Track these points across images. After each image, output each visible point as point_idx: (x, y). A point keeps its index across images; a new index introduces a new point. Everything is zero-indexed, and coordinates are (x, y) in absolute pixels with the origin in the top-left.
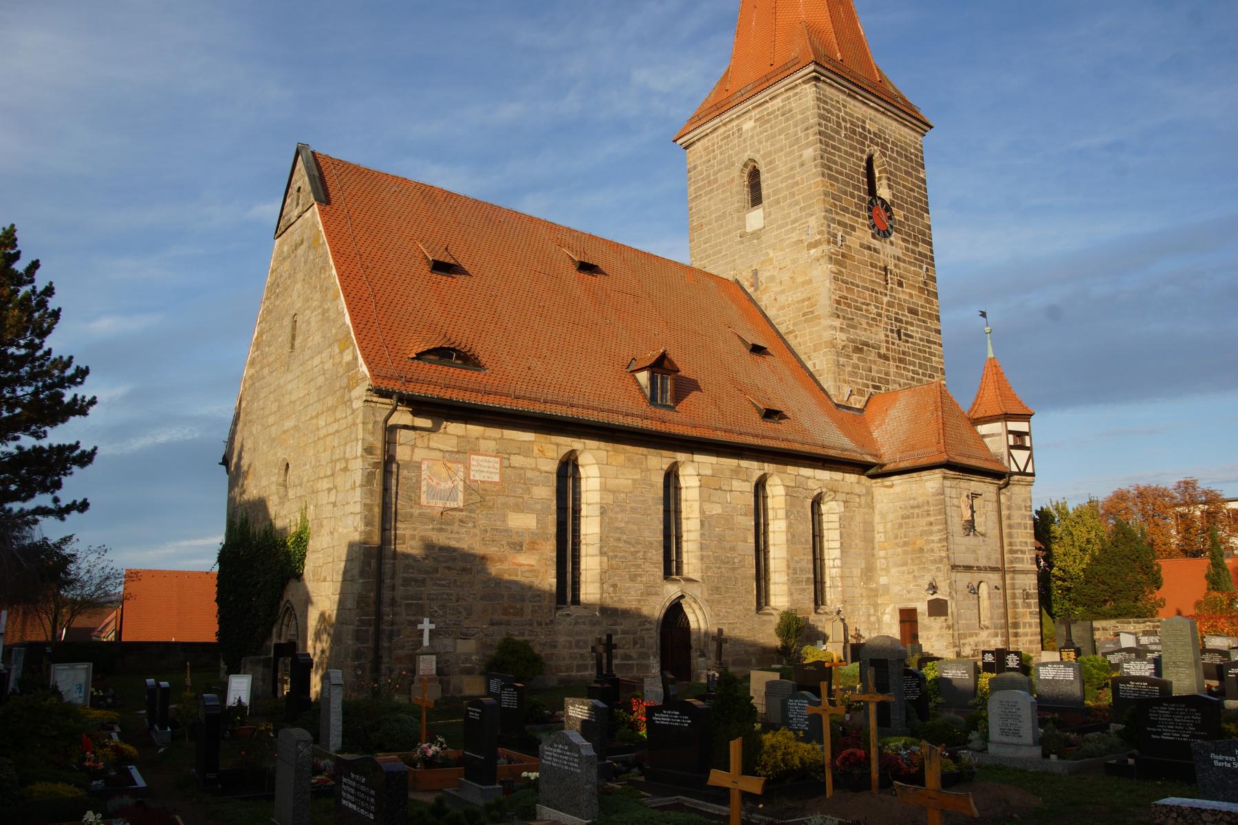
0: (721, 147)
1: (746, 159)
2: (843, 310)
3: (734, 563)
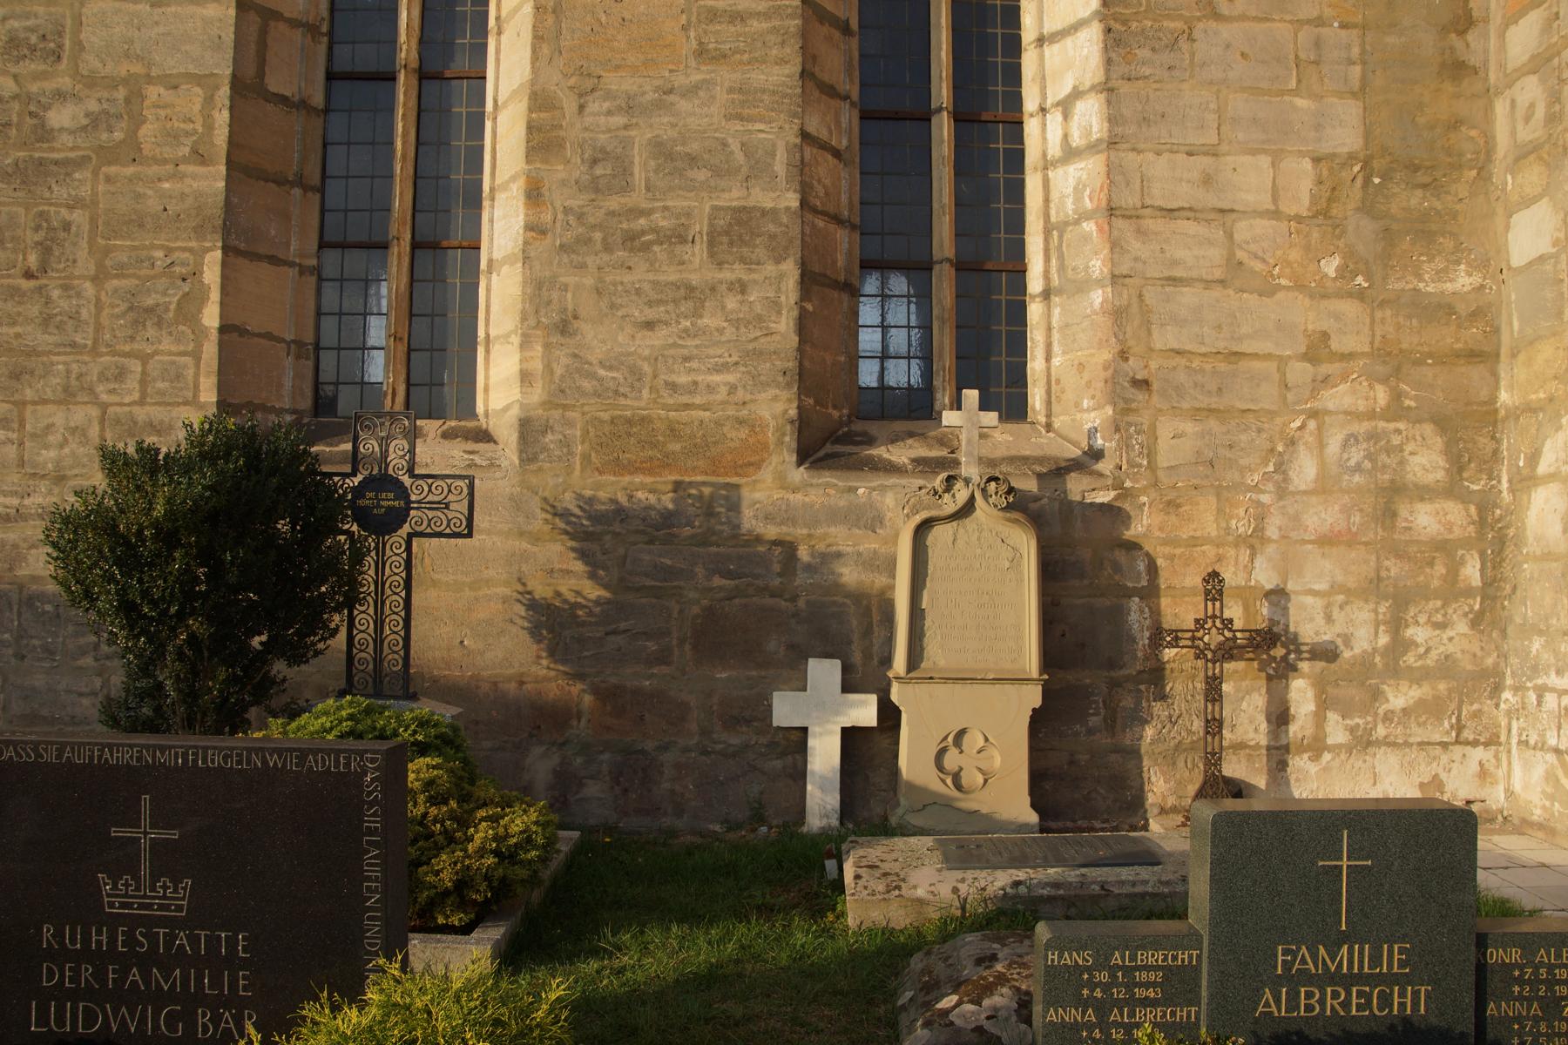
3: (44, 134)
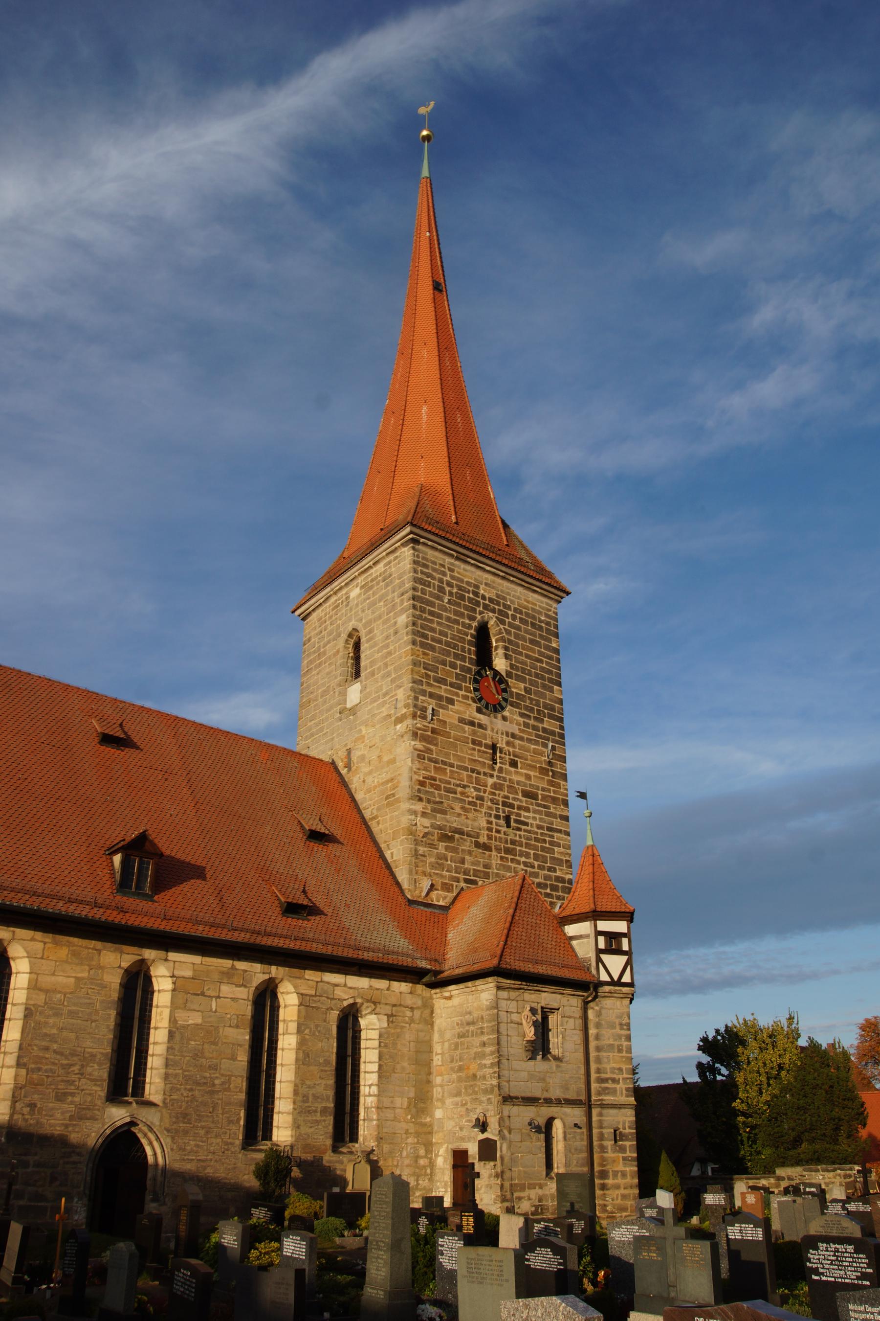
0: (331, 617)
1: (350, 629)
2: (427, 792)
3: (214, 1085)
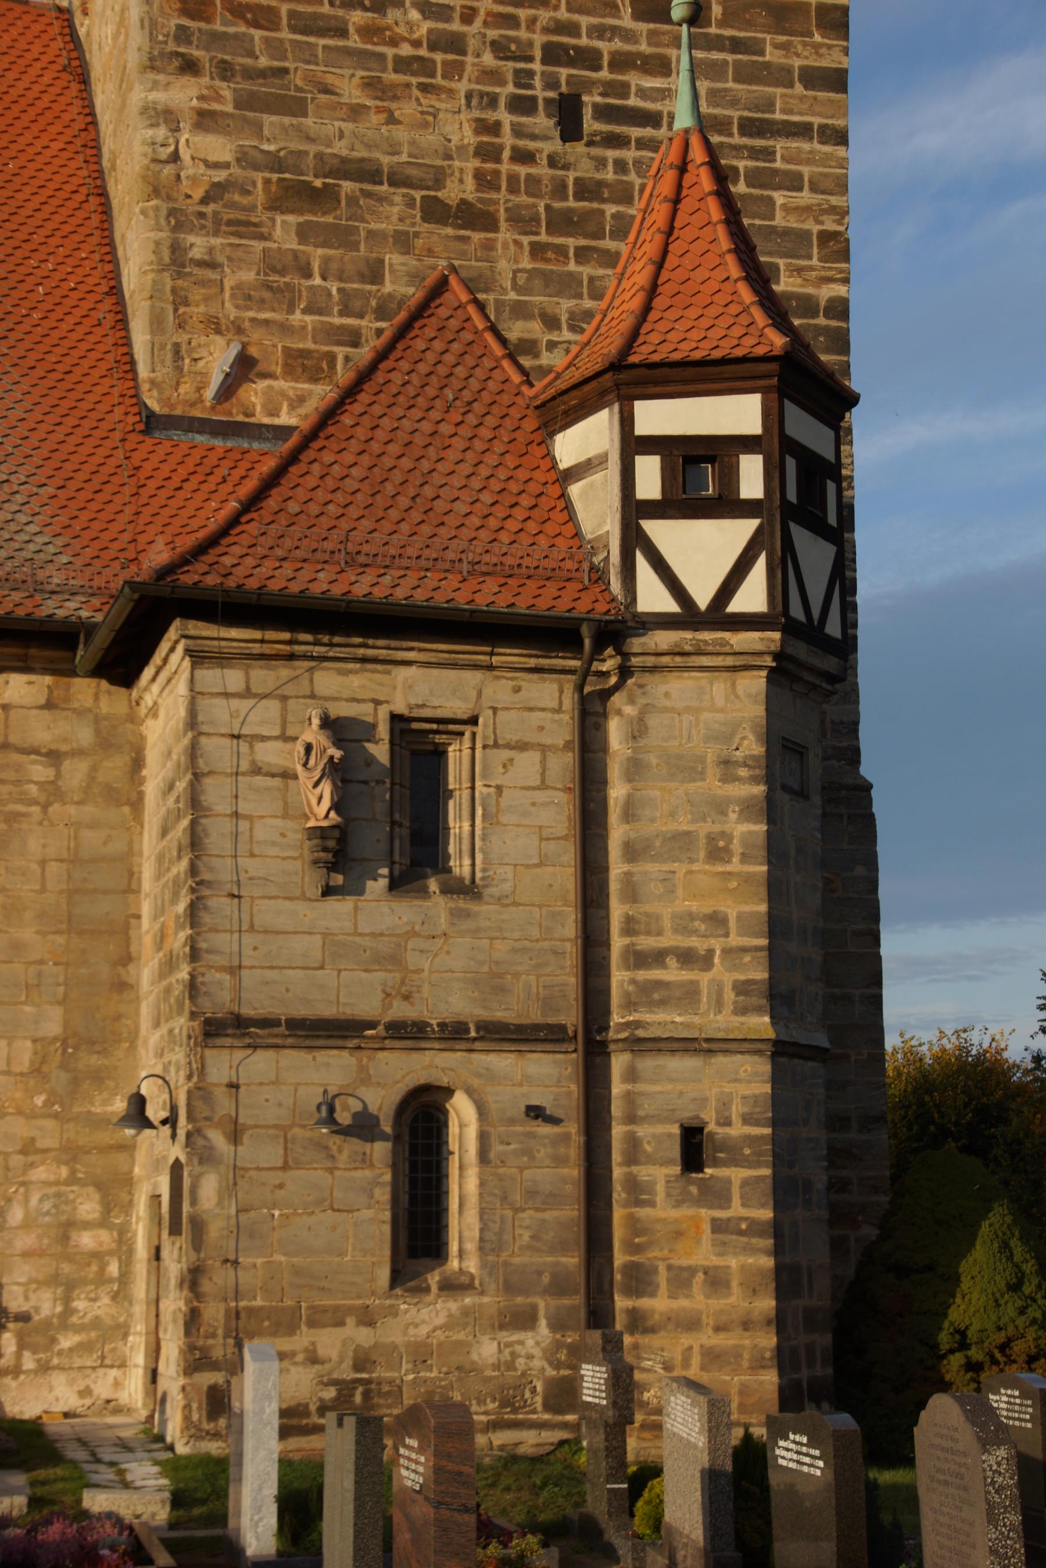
2: (216, 38)
